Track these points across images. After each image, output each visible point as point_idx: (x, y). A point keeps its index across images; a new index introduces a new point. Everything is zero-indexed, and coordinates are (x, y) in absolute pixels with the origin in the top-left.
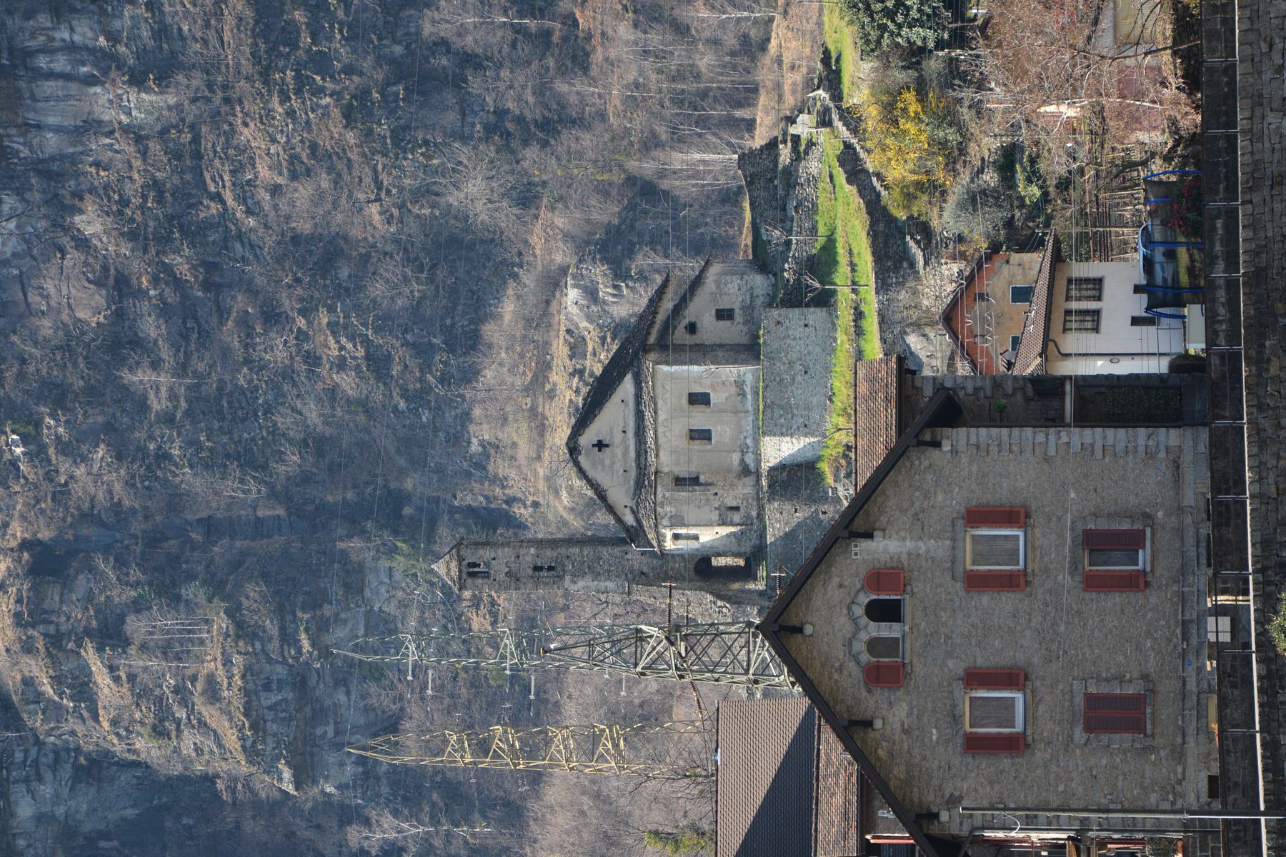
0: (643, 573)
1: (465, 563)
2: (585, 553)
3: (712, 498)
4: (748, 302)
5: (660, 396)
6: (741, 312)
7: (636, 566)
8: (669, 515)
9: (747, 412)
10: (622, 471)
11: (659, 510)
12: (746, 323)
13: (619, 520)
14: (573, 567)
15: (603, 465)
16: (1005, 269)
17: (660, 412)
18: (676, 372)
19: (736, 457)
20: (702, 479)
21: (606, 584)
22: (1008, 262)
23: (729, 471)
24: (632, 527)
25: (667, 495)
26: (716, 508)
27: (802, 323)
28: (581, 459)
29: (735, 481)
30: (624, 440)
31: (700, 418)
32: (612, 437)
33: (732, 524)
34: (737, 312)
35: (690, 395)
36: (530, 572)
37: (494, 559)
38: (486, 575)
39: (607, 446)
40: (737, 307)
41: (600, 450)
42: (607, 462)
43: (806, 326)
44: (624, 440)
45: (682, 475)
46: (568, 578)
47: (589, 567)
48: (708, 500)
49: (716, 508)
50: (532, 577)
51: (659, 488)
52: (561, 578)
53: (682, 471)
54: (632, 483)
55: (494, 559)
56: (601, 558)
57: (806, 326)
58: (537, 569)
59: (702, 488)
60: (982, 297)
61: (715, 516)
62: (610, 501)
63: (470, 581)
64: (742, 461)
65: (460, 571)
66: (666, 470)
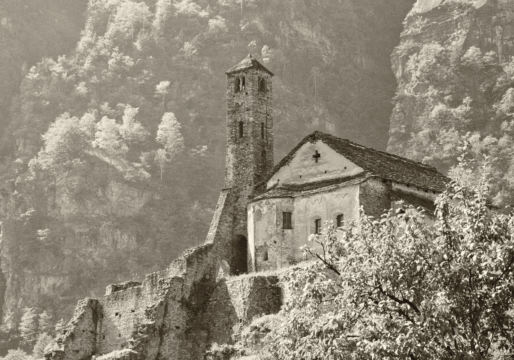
0: (238, 198)
1: (244, 74)
2: (250, 156)
3: (273, 239)
5: (340, 193)
7: (242, 193)
8: (261, 209)
10: (300, 174)
11: (264, 201)
13: (269, 177)
14: (242, 149)
15: (304, 160)
17: (330, 194)
18: (355, 202)
21: (231, 173)
24: (265, 187)
25: (275, 207)
26: (265, 243)
28: (308, 144)
29: (286, 256)
30: (322, 173)
32: (321, 164)
33: (256, 255)
35: (342, 215)
36: (239, 120)
37: (247, 94)
38: (237, 90)
41: (314, 156)
42: (306, 163)
44: (322, 173)
45: (293, 217)
46: (235, 146)
47: (241, 160)
48: (271, 236)
49: (265, 243)
50: (235, 122)
51: (279, 200)
53: (295, 217)
54: (293, 183)
55: (247, 94)
58: (241, 124)
61: (261, 243)
62: (282, 169)
65: (239, 72)
66: (295, 205)
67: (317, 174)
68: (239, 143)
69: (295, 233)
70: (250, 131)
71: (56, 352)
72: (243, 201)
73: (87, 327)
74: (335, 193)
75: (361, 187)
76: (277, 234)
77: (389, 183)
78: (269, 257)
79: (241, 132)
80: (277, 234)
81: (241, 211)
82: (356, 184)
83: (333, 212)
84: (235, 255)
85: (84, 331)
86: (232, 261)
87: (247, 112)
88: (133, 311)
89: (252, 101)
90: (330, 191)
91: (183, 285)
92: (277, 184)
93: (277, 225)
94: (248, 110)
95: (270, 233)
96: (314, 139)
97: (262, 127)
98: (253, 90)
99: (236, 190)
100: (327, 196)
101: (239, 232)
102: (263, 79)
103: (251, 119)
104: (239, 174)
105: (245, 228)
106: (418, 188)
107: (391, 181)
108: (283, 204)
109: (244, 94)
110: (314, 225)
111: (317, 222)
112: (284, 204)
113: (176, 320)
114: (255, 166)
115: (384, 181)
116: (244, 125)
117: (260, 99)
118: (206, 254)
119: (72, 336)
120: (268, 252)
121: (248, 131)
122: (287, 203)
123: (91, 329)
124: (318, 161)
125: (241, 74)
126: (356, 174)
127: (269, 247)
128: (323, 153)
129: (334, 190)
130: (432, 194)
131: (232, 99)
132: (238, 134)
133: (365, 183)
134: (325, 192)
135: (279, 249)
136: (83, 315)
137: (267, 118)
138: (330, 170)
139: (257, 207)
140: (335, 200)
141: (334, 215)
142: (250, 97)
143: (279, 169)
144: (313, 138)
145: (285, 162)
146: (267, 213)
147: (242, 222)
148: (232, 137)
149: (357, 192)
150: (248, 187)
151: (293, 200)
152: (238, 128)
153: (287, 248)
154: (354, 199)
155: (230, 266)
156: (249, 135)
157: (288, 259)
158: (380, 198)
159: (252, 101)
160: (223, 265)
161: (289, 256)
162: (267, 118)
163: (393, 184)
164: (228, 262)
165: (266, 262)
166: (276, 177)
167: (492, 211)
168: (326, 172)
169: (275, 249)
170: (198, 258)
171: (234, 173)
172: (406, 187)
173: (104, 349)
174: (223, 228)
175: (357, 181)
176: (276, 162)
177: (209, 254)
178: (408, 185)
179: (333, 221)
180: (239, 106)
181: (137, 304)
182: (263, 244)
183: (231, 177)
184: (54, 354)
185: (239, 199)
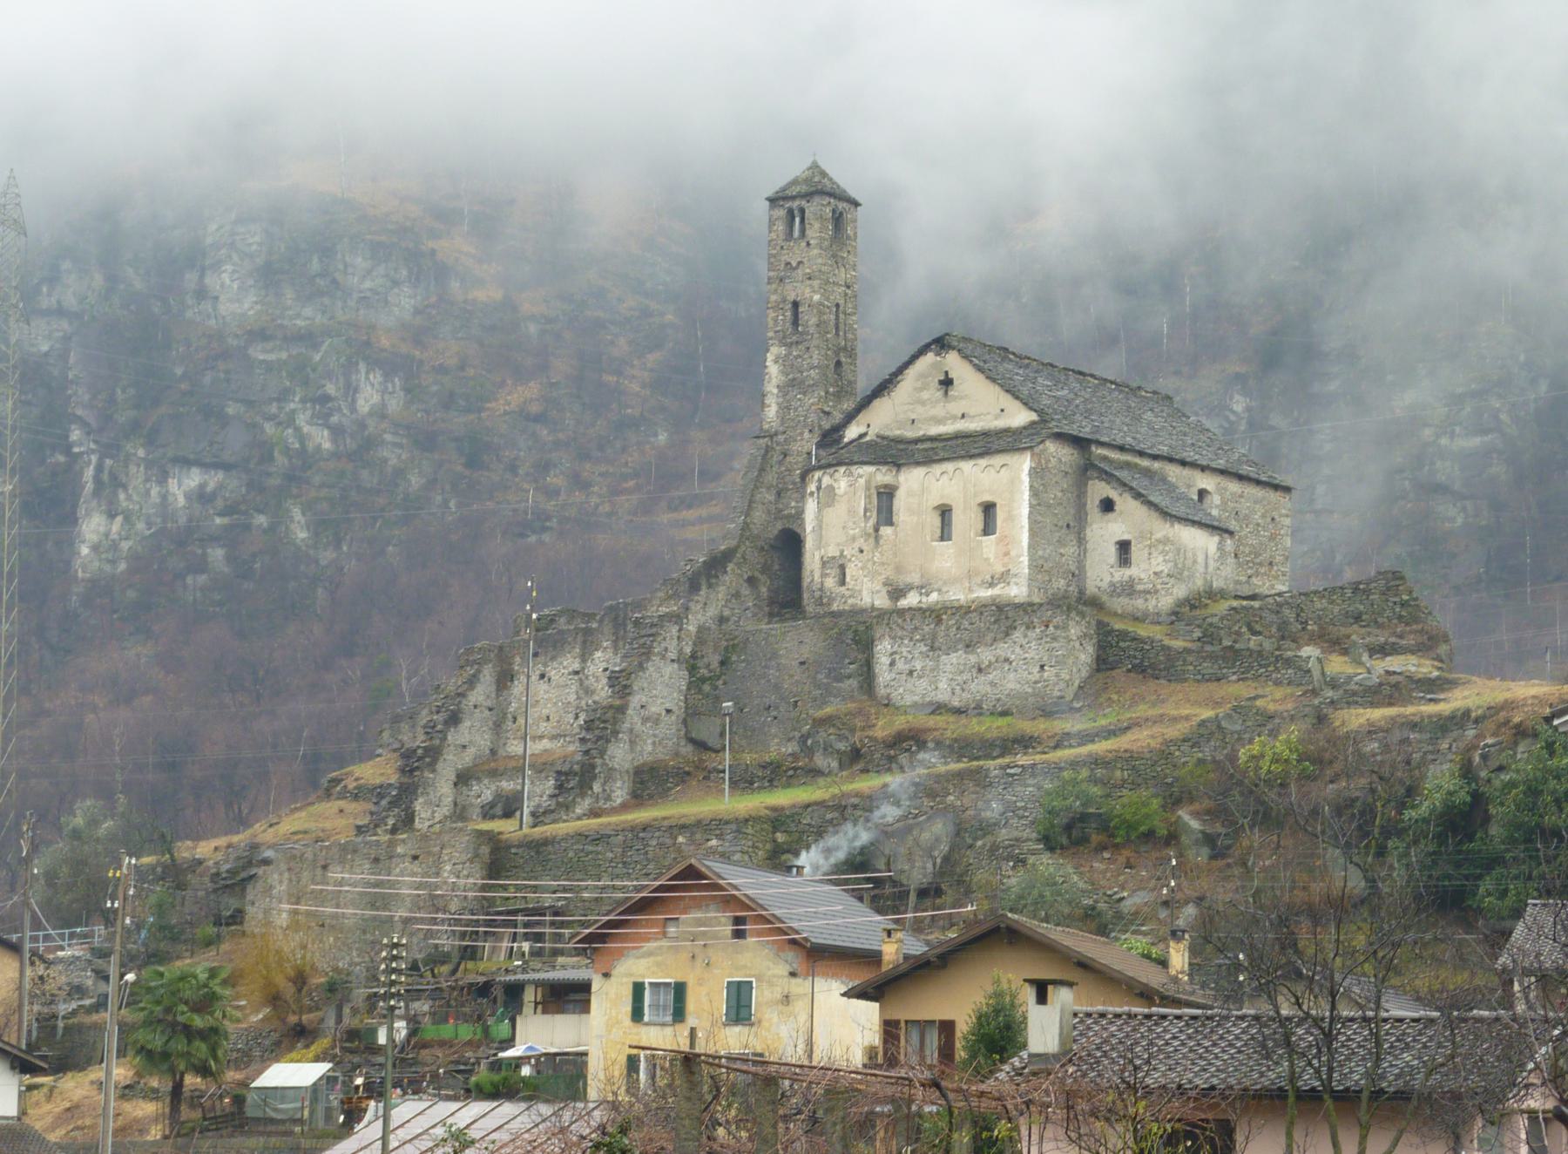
1: (803, 203)
3: (857, 545)
4: (1139, 587)
6: (1126, 578)
7: (795, 447)
8: (836, 485)
9: (971, 590)
10: (913, 416)
13: (850, 418)
14: (799, 356)
15: (921, 389)
16: (782, 970)
17: (972, 462)
18: (1021, 482)
19: (915, 578)
20: (886, 531)
22: (793, 974)
24: (842, 437)
25: (862, 481)
28: (930, 358)
29: (882, 578)
30: (954, 418)
31: (966, 520)
32: (955, 398)
33: (824, 575)
36: (791, 297)
39: (946, 393)
41: (941, 382)
42: (925, 395)
43: (1042, 667)
46: (783, 351)
47: (794, 379)
48: (854, 539)
49: (842, 551)
51: (871, 469)
52: (782, 343)
53: (900, 502)
54: (898, 432)
55: (808, 244)
57: (1042, 667)
58: (796, 305)
59: (871, 531)
60: (739, 934)
61: (832, 551)
62: (877, 403)
63: (781, 213)
64: (910, 588)
65: (793, 198)
67: (947, 419)
68: (792, 344)
70: (814, 321)
71: (425, 748)
79: (796, 322)
87: (808, 282)
88: (577, 673)
91: (680, 630)
92: (865, 434)
94: (810, 279)
95: (851, 532)
98: (821, 238)
102: (841, 214)
103: (816, 297)
104: (787, 408)
106: (1141, 454)
109: (804, 244)
110: (937, 521)
111: (945, 512)
112: (883, 476)
114: (823, 394)
116: (800, 310)
117: (834, 256)
121: (809, 319)
122: (885, 475)
123: (489, 703)
124: (950, 393)
125: (795, 204)
127: (850, 560)
133: (1041, 446)
135: (869, 565)
137: (846, 295)
138: (972, 412)
141: (979, 505)
144: (941, 344)
145: (883, 388)
146: (846, 493)
147: (793, 504)
150: (806, 435)
151: (898, 471)
152: (788, 314)
153: (883, 564)
157: (885, 584)
161: (887, 578)
163: (1093, 448)
168: (963, 416)
170: (709, 577)
176: (863, 385)
177: (730, 567)
178: (1122, 448)
179: (977, 519)
182: (838, 554)
183: (772, 412)
184: (420, 752)
185: (789, 459)
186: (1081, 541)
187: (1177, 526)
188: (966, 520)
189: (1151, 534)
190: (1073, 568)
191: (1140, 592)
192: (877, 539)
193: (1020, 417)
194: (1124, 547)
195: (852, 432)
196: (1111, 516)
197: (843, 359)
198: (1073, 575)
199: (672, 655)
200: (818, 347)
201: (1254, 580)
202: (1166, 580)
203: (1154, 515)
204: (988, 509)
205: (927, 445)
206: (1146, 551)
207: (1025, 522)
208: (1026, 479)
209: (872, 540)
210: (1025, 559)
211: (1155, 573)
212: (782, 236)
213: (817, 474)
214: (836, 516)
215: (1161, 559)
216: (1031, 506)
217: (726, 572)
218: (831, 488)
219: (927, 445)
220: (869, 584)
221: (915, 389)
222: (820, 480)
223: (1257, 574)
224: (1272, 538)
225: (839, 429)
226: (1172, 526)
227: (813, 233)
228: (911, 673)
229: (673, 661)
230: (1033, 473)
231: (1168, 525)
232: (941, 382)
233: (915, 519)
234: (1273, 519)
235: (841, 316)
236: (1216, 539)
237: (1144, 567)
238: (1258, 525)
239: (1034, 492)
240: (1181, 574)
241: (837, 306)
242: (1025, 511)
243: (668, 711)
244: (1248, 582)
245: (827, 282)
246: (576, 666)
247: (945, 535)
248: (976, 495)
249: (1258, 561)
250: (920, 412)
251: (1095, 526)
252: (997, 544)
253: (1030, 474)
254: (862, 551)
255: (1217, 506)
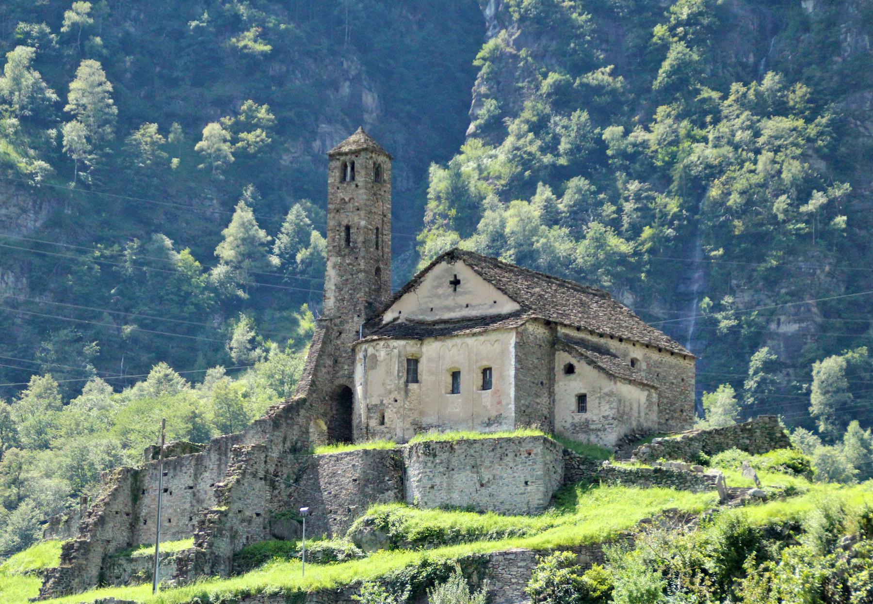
1: (353, 157)
3: (392, 396)
4: (592, 427)
5: (488, 338)
6: (583, 420)
7: (347, 327)
8: (377, 354)
10: (432, 306)
11: (382, 343)
12: (574, 425)
13: (387, 307)
14: (349, 264)
15: (437, 287)
17: (474, 339)
18: (509, 352)
20: (413, 386)
23: (422, 413)
24: (381, 320)
25: (396, 351)
26: (382, 401)
27: (529, 478)
28: (443, 265)
29: (410, 420)
30: (461, 307)
31: (470, 380)
32: (462, 293)
33: (368, 418)
34: (584, 416)
35: (490, 369)
36: (345, 223)
37: (357, 186)
38: (343, 179)
39: (455, 290)
40: (588, 415)
41: (451, 283)
42: (440, 291)
43: (526, 483)
44: (461, 307)
46: (339, 260)
47: (347, 280)
48: (390, 392)
49: (382, 401)
50: (340, 225)
52: (339, 253)
53: (423, 367)
54: (421, 317)
55: (357, 186)
56: (354, 290)
57: (526, 483)
58: (348, 228)
59: (402, 386)
61: (375, 401)
62: (405, 296)
65: (346, 154)
69: (424, 389)
70: (361, 239)
71: (80, 543)
72: (348, 339)
73: (121, 507)
74: (482, 338)
75: (517, 333)
76: (398, 389)
77: (553, 325)
78: (386, 420)
79: (348, 240)
80: (398, 389)
81: (346, 352)
82: (511, 329)
83: (479, 364)
84: (334, 412)
85: (117, 513)
86: (331, 421)
88: (191, 488)
89: (365, 197)
90: (474, 335)
91: (266, 456)
92: (398, 318)
93: (399, 378)
95: (388, 387)
96: (452, 258)
97: (377, 232)
98: (367, 182)
99: (338, 321)
100: (471, 341)
101: (342, 381)
102: (379, 165)
103: (363, 223)
104: (343, 300)
105: (351, 376)
106: (592, 332)
107: (556, 323)
108: (408, 348)
109: (353, 186)
110: (449, 380)
111: (456, 375)
113: (256, 505)
114: (367, 290)
115: (547, 323)
116: (351, 231)
117: (375, 194)
118: (298, 412)
119: (102, 521)
120: (386, 414)
121: (358, 238)
122: (412, 346)
123: (127, 510)
124: (458, 289)
125: (349, 157)
126: (509, 311)
127: (387, 407)
128: (464, 279)
129: (480, 334)
130: (609, 339)
131: (336, 192)
132: (343, 243)
133: (523, 327)
134: (468, 335)
135: (401, 410)
136: (116, 490)
138: (473, 303)
139: (371, 351)
140: (481, 348)
142: (362, 191)
143: (401, 296)
147: (346, 367)
148: (334, 247)
149: (512, 339)
150: (356, 319)
151: (421, 344)
152: (343, 234)
153: (411, 409)
154: (508, 349)
155: (329, 428)
156: (360, 245)
157: (412, 424)
158: (540, 346)
159: (365, 197)
160: (318, 425)
161: (414, 420)
162: (383, 221)
163: (559, 328)
164: (326, 423)
165: (382, 427)
166: (396, 307)
167: (686, 361)
168: (467, 306)
169: (395, 410)
171: (336, 297)
172: (576, 331)
173: (145, 538)
174: (319, 374)
175: (512, 324)
177: (302, 412)
178: (578, 329)
180: (345, 203)
181: (195, 477)
184: (76, 545)
185: (343, 335)
186: (551, 394)
187: (619, 384)
188: (470, 380)
189: (601, 389)
190: (545, 412)
191: (593, 430)
192: (407, 391)
193: (509, 306)
194: (582, 399)
195: (388, 317)
196: (572, 376)
197: (382, 266)
198: (546, 418)
199: (261, 474)
200: (364, 257)
201: (670, 422)
202: (611, 421)
203: (603, 375)
204: (486, 372)
205: (442, 326)
206: (597, 401)
207: (512, 380)
208: (512, 350)
209: (403, 393)
210: (512, 407)
211: (604, 417)
212: (338, 180)
213: (364, 346)
214: (377, 375)
215: (607, 406)
216: (516, 369)
217: (299, 415)
218: (374, 356)
219: (442, 326)
220: (401, 424)
221: (433, 287)
222: (366, 350)
223: (672, 418)
224: (682, 393)
225: (379, 315)
226: (615, 383)
227: (360, 179)
228: (432, 487)
229: (261, 479)
230: (518, 345)
231: (612, 383)
232: (451, 283)
233: (434, 378)
234: (683, 380)
235: (380, 236)
236: (646, 393)
237: (596, 412)
238: (673, 383)
239: (518, 360)
240: (622, 417)
241: (377, 229)
242: (512, 372)
243: (258, 515)
244: (666, 424)
245: (370, 212)
246: (191, 483)
247: (455, 390)
248: (477, 361)
249: (672, 408)
250: (436, 303)
251: (561, 383)
252: (493, 396)
253: (516, 347)
254: (396, 401)
255: (644, 370)
